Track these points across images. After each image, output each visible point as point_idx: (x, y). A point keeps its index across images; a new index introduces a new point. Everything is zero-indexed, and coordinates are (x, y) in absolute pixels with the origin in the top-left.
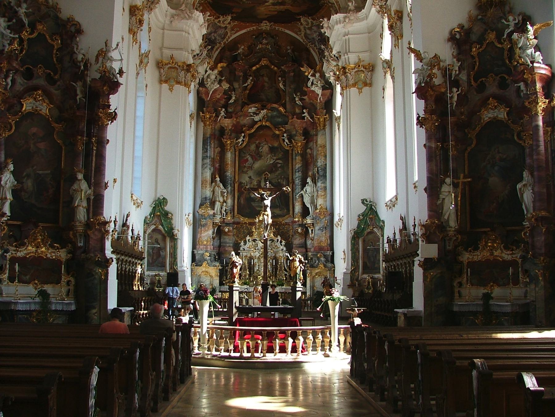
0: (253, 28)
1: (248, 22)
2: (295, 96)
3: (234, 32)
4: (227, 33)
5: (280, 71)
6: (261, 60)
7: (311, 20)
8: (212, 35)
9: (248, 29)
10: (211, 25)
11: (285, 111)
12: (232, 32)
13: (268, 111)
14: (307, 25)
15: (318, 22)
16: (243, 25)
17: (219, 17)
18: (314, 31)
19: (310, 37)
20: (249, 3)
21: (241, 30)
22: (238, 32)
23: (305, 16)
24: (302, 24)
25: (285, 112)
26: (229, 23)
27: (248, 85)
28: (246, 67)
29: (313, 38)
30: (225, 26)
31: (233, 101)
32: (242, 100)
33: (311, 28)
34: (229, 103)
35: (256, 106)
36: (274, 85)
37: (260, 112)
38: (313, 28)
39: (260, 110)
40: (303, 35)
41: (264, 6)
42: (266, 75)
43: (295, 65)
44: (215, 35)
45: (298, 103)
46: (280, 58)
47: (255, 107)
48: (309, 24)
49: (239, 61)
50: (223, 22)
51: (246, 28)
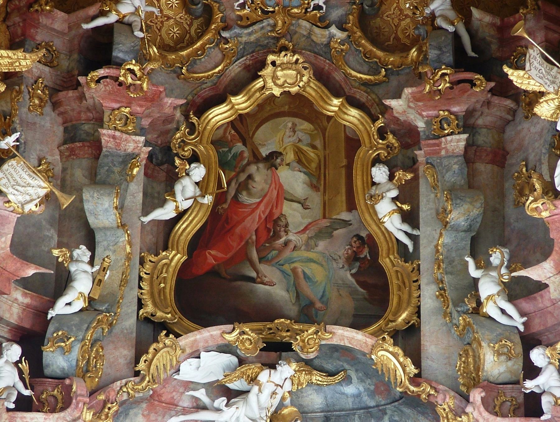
2: (474, 272)
5: (382, 133)
6: (262, 65)
11: (412, 369)
13: (304, 378)
25: (416, 379)
27: (181, 215)
28: (169, 101)
31: (79, 305)
32: (140, 305)
34: (51, 314)
35: (231, 338)
36: (345, 216)
37: (253, 380)
39: (251, 369)
42: (290, 156)
43: (473, 85)
45: (490, 309)
46: (379, 53)
47: (225, 349)
49: (119, 65)
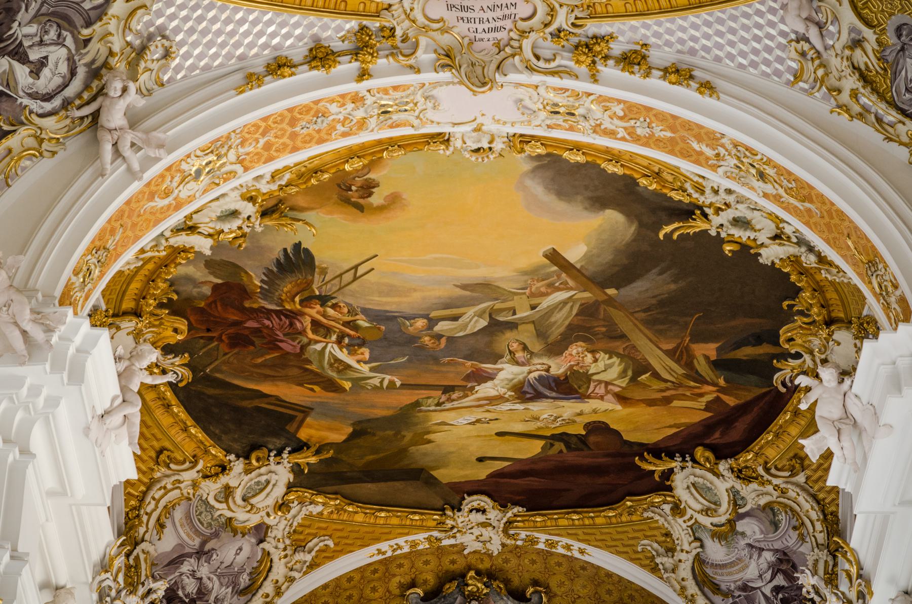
0: (414, 544)
1: (383, 503)
3: (308, 558)
4: (264, 566)
7: (731, 482)
8: (185, 568)
9: (384, 546)
10: (178, 514)
12: (300, 556)
14: (706, 512)
15: (770, 488)
16: (359, 518)
17: (224, 468)
18: (750, 546)
19: (727, 580)
20: (392, 384)
21: (341, 551)
22: (331, 558)
23: (694, 461)
24: (677, 509)
26: (282, 506)
29: (745, 588)
30: (254, 520)
33: (733, 529)
38: (740, 526)
40: (685, 571)
41: (467, 402)
44: (204, 571)
48: (717, 504)
50: (244, 500)
51: (378, 540)
